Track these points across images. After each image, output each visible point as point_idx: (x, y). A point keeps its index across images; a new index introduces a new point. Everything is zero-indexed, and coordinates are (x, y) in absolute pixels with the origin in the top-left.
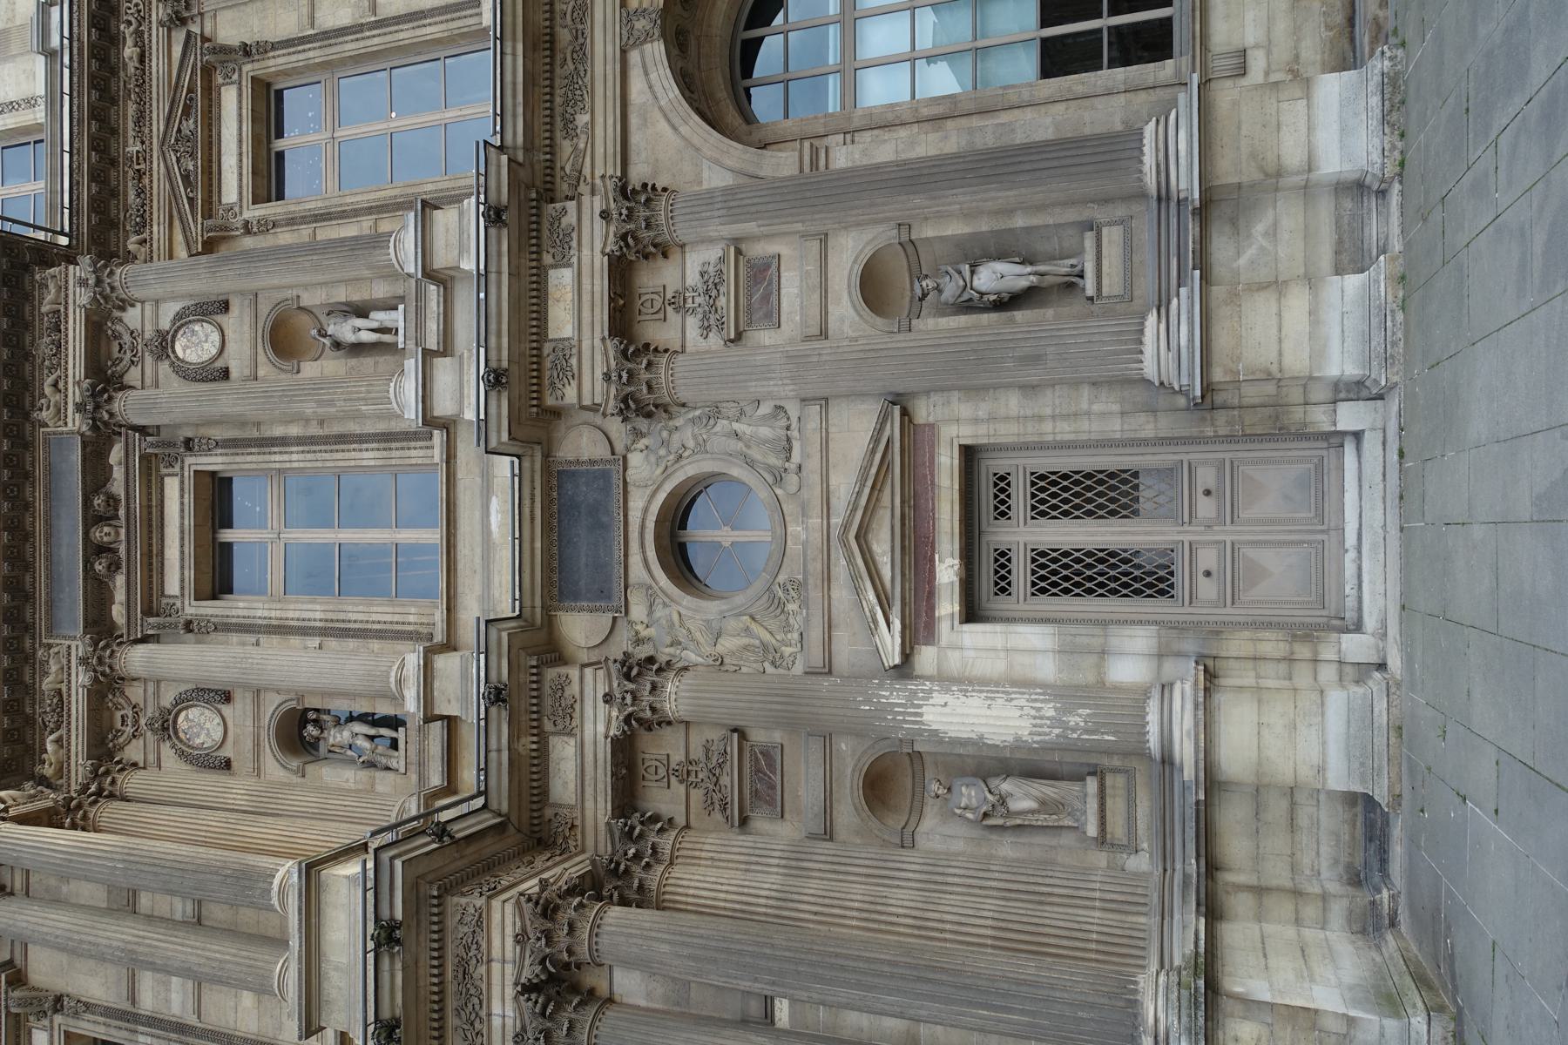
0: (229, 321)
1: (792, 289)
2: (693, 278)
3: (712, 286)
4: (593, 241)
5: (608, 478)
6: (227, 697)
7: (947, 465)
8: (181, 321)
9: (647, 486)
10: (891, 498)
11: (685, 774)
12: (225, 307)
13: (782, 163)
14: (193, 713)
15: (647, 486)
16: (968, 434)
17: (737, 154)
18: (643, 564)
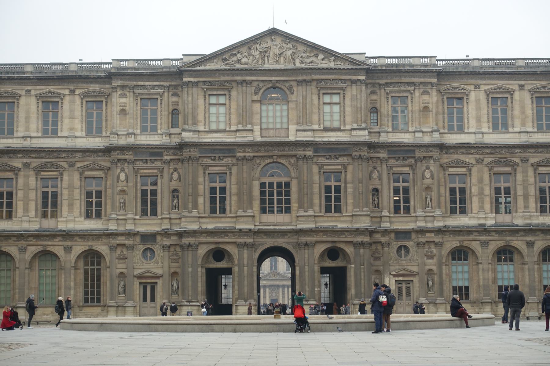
0: (430, 180)
1: (430, 261)
2: (432, 249)
3: (431, 252)
4: (437, 239)
5: (409, 238)
6: (379, 180)
7: (412, 278)
8: (431, 171)
9: (409, 244)
10: (408, 273)
11: (376, 249)
12: (433, 179)
13: (444, 261)
14: (377, 173)
15: (409, 244)
16: (414, 281)
17: (446, 254)
18: (400, 243)
